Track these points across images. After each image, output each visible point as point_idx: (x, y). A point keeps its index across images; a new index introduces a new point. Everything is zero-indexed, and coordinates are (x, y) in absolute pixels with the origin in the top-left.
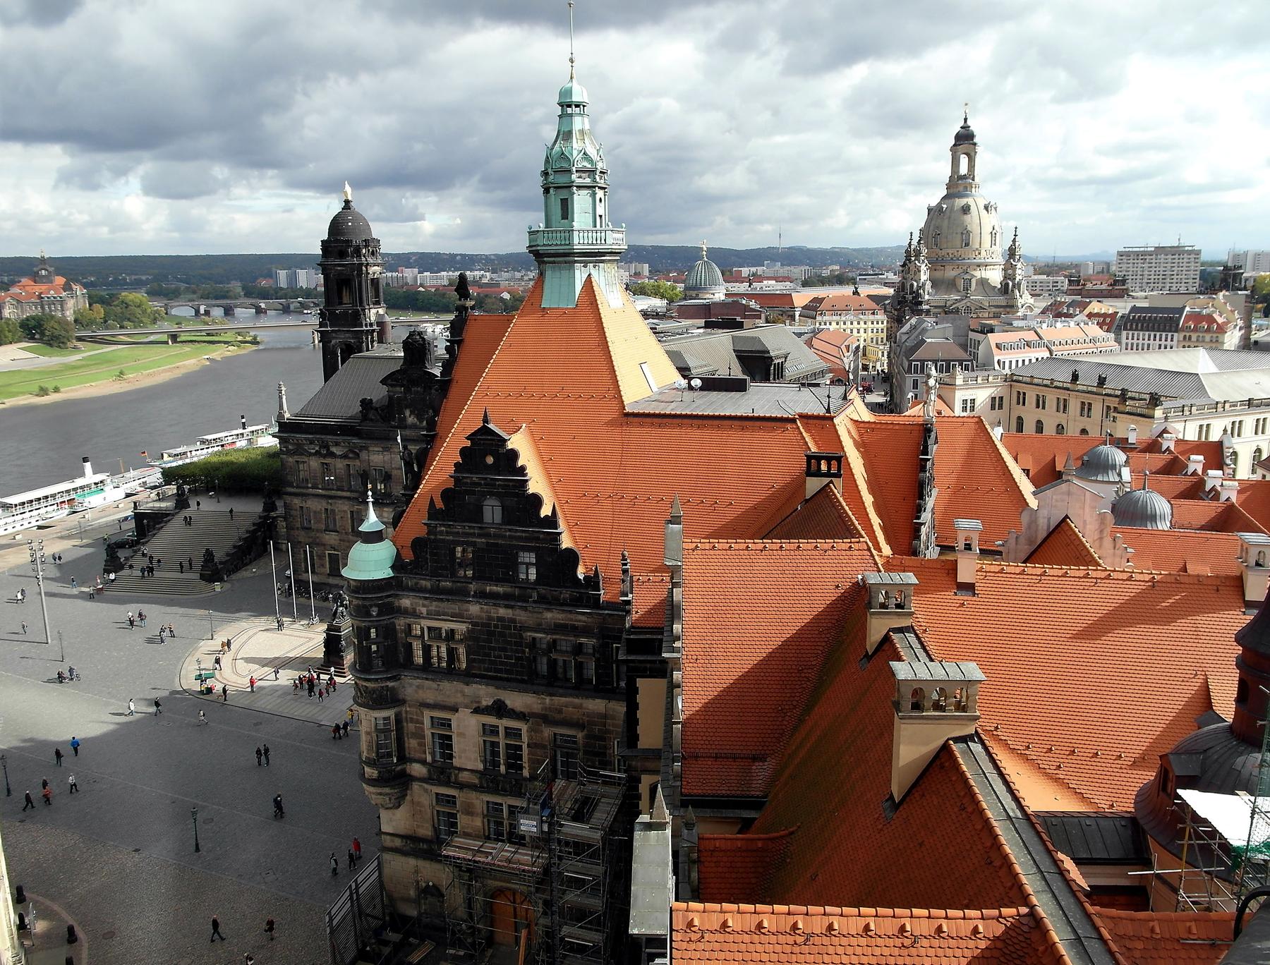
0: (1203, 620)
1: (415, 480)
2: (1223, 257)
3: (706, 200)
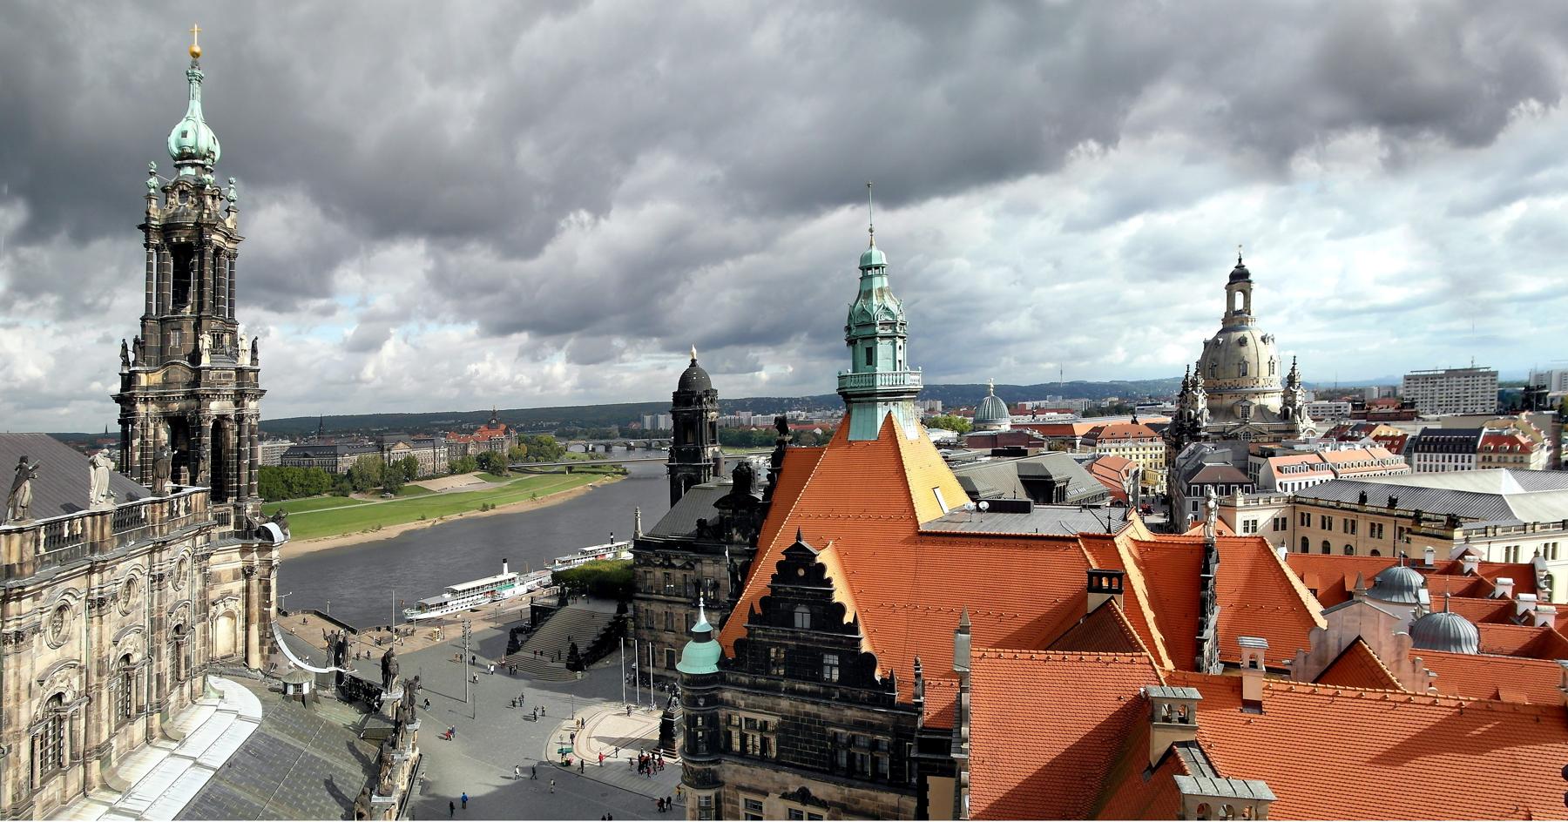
0: (1524, 753)
1: (739, 588)
2: (1525, 378)
3: (995, 344)
